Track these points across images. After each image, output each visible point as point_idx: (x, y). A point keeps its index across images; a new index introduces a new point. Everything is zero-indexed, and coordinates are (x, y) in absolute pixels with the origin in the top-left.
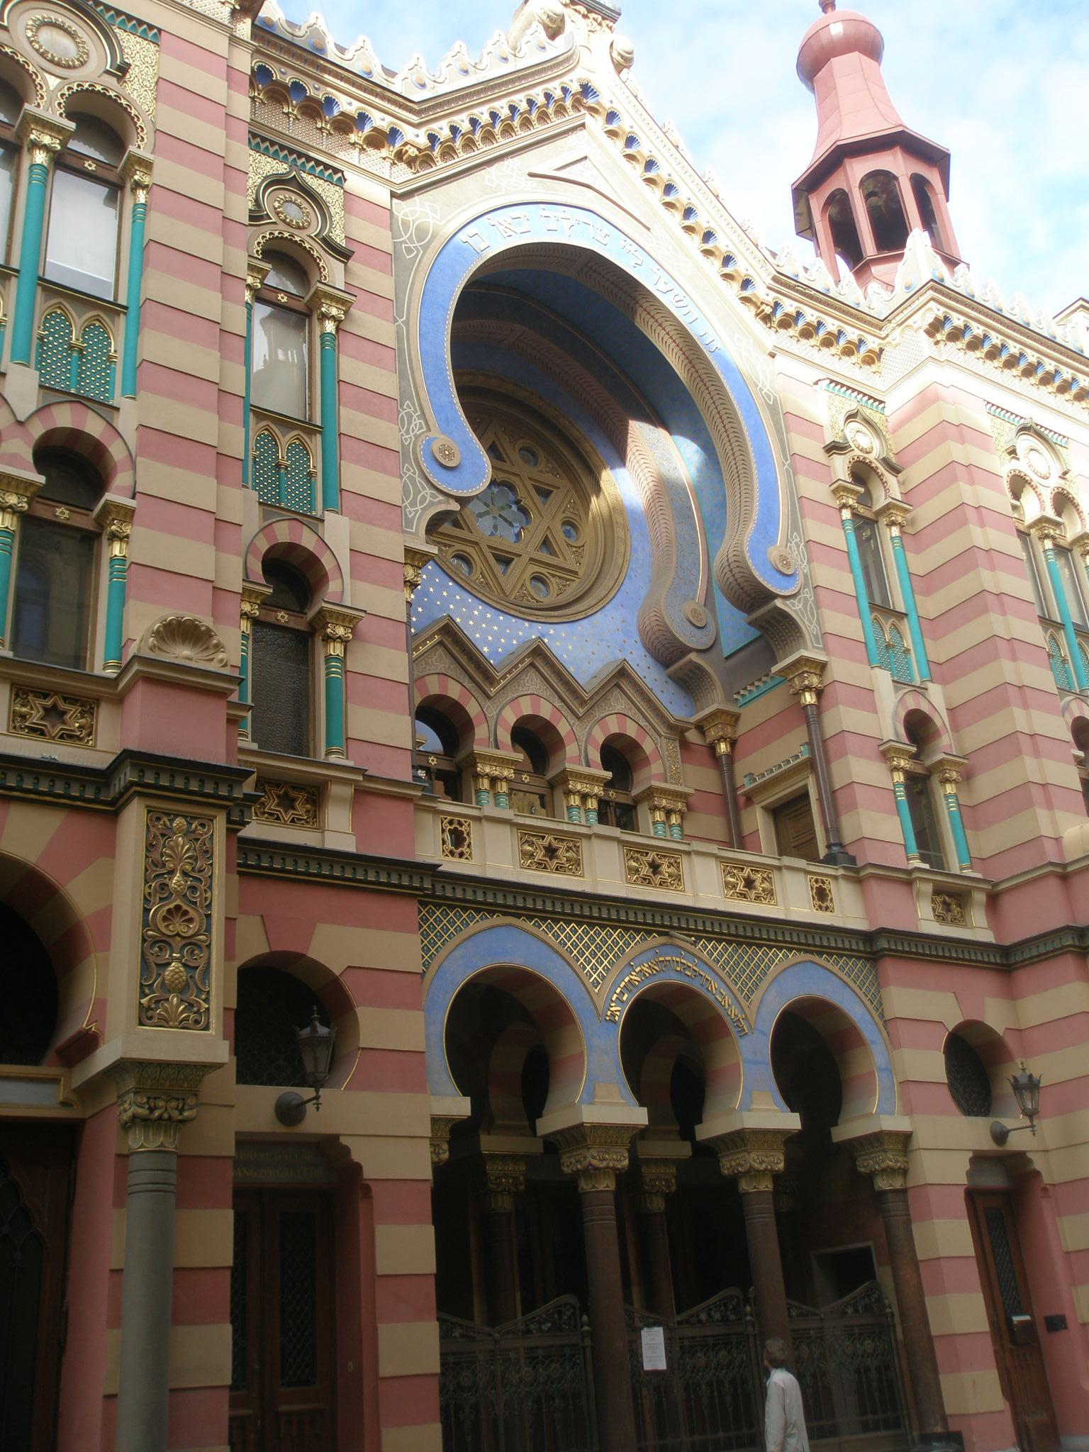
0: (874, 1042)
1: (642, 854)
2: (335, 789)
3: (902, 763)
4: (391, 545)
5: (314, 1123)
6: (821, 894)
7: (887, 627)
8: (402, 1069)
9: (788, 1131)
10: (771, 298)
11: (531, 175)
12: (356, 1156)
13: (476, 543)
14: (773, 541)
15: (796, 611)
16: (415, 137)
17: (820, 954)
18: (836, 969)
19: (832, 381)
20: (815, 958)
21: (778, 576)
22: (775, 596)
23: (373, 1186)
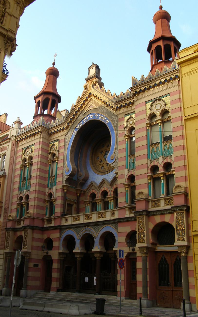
0: (116, 237)
1: (87, 215)
2: (52, 219)
3: (126, 186)
4: (60, 187)
5: (49, 254)
6: (113, 214)
7: (133, 158)
8: (58, 248)
9: (98, 252)
10: (116, 106)
11: (83, 115)
12: (52, 257)
13: (104, 164)
14: (112, 154)
15: (114, 165)
16: (65, 126)
17: (109, 224)
18: (112, 226)
19: (125, 115)
20: (109, 225)
21: (111, 160)
22: (111, 164)
23: (53, 260)
